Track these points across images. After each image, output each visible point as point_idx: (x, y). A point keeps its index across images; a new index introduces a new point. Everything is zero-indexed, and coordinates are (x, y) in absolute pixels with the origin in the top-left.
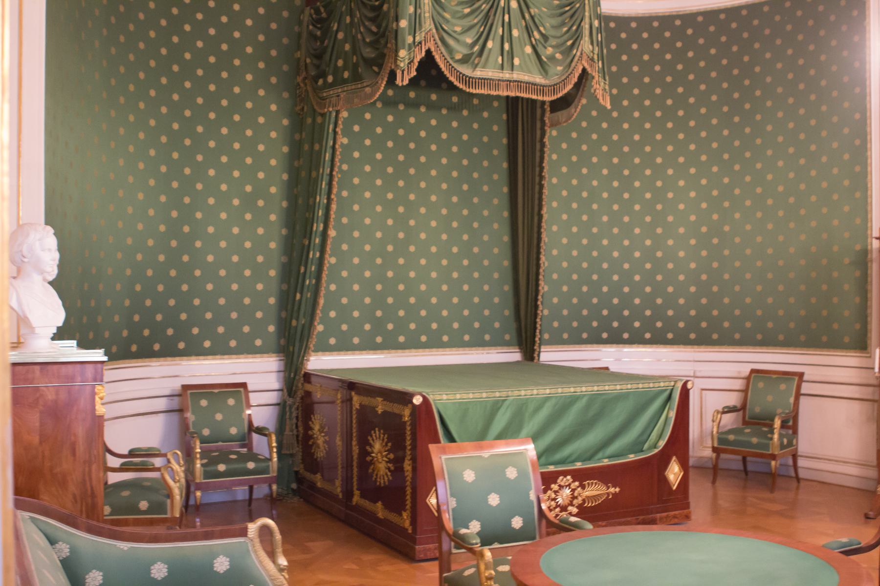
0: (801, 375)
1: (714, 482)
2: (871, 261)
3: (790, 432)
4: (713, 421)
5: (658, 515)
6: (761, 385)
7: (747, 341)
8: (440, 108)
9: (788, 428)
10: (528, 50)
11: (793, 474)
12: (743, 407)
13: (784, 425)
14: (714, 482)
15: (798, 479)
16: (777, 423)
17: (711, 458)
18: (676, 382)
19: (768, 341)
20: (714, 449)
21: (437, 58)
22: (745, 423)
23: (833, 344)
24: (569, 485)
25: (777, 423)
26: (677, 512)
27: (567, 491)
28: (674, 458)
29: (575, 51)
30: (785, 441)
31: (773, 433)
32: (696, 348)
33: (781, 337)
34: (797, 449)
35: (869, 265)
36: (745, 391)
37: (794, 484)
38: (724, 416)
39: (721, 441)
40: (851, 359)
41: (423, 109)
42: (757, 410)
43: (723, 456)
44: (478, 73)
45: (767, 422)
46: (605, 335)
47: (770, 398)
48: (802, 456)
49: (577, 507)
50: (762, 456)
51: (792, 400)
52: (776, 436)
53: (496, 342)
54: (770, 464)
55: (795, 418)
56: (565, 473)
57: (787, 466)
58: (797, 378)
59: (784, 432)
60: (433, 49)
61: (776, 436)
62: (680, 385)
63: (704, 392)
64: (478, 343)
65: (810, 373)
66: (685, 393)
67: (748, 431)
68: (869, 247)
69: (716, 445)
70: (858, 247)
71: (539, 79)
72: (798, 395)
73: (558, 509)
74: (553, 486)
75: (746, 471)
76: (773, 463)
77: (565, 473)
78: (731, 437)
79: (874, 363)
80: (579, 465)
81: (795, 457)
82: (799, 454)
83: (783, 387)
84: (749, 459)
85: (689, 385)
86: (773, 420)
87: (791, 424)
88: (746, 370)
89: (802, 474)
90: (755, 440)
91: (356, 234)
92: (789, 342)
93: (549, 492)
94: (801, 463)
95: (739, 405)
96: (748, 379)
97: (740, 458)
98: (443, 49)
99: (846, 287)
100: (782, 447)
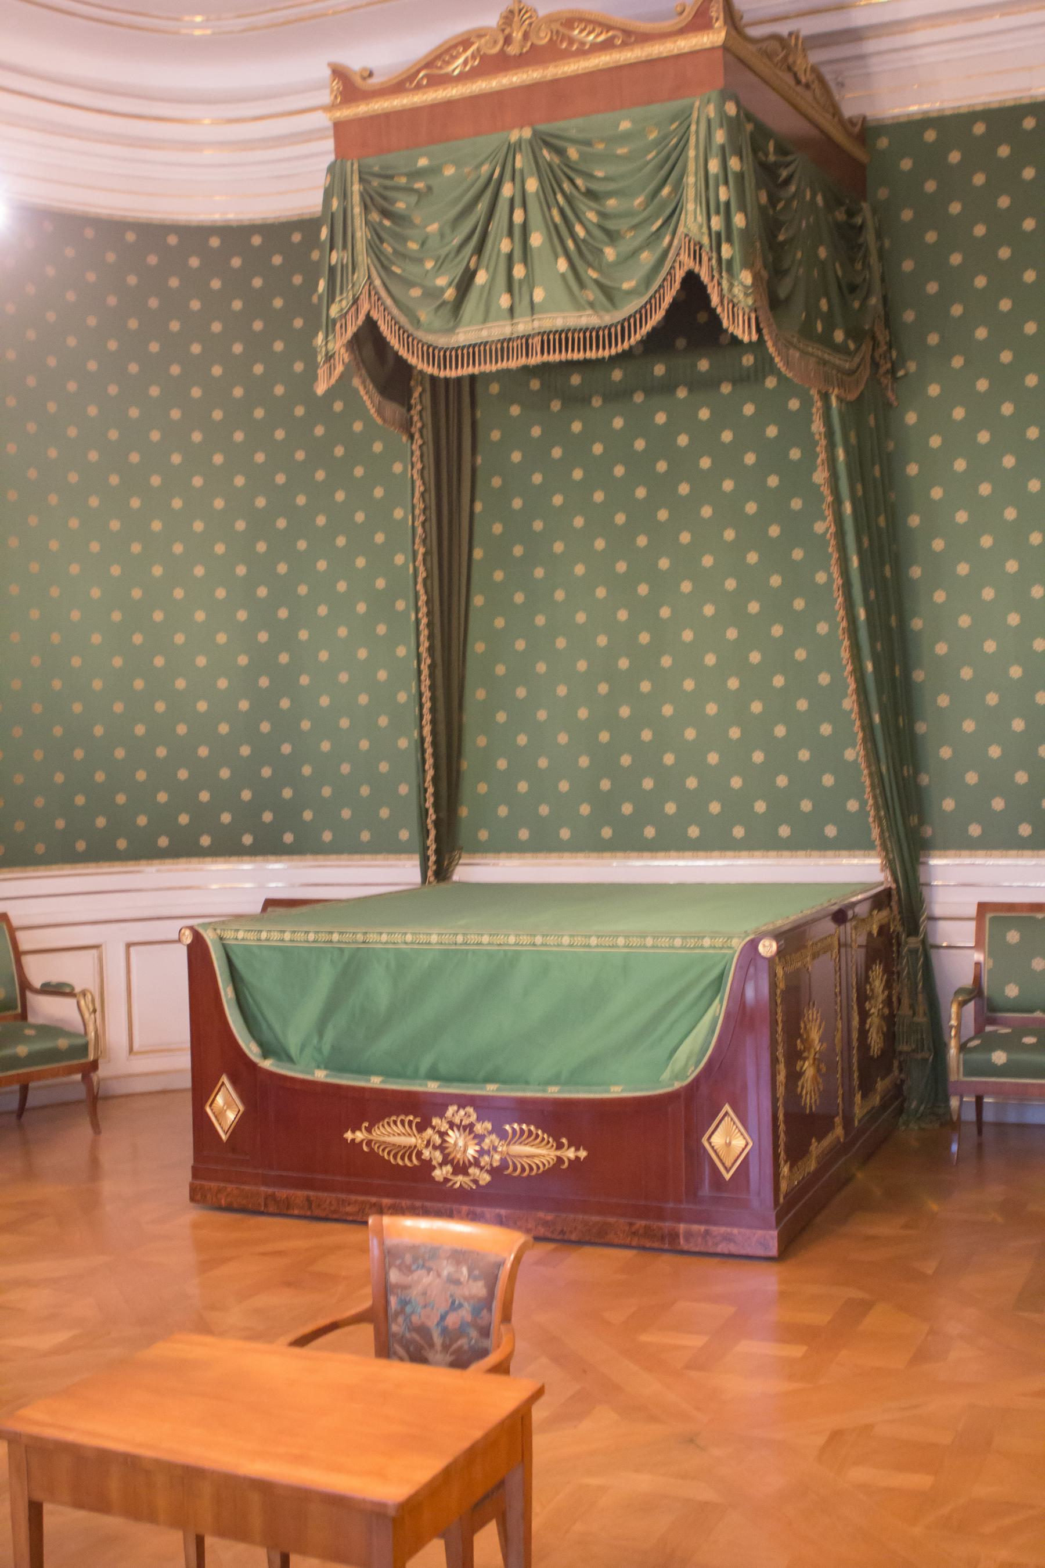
5: (682, 1227)
8: (718, 385)
10: (562, 265)
21: (384, 328)
24: (471, 1126)
26: (735, 1231)
27: (453, 1137)
29: (667, 240)
41: (682, 393)
44: (464, 336)
46: (163, 842)
49: (487, 1171)
53: (851, 842)
60: (375, 315)
64: (808, 840)
71: (587, 319)
73: (449, 1168)
74: (435, 1121)
77: (463, 1101)
91: (561, 643)
93: (429, 1131)
98: (395, 311)
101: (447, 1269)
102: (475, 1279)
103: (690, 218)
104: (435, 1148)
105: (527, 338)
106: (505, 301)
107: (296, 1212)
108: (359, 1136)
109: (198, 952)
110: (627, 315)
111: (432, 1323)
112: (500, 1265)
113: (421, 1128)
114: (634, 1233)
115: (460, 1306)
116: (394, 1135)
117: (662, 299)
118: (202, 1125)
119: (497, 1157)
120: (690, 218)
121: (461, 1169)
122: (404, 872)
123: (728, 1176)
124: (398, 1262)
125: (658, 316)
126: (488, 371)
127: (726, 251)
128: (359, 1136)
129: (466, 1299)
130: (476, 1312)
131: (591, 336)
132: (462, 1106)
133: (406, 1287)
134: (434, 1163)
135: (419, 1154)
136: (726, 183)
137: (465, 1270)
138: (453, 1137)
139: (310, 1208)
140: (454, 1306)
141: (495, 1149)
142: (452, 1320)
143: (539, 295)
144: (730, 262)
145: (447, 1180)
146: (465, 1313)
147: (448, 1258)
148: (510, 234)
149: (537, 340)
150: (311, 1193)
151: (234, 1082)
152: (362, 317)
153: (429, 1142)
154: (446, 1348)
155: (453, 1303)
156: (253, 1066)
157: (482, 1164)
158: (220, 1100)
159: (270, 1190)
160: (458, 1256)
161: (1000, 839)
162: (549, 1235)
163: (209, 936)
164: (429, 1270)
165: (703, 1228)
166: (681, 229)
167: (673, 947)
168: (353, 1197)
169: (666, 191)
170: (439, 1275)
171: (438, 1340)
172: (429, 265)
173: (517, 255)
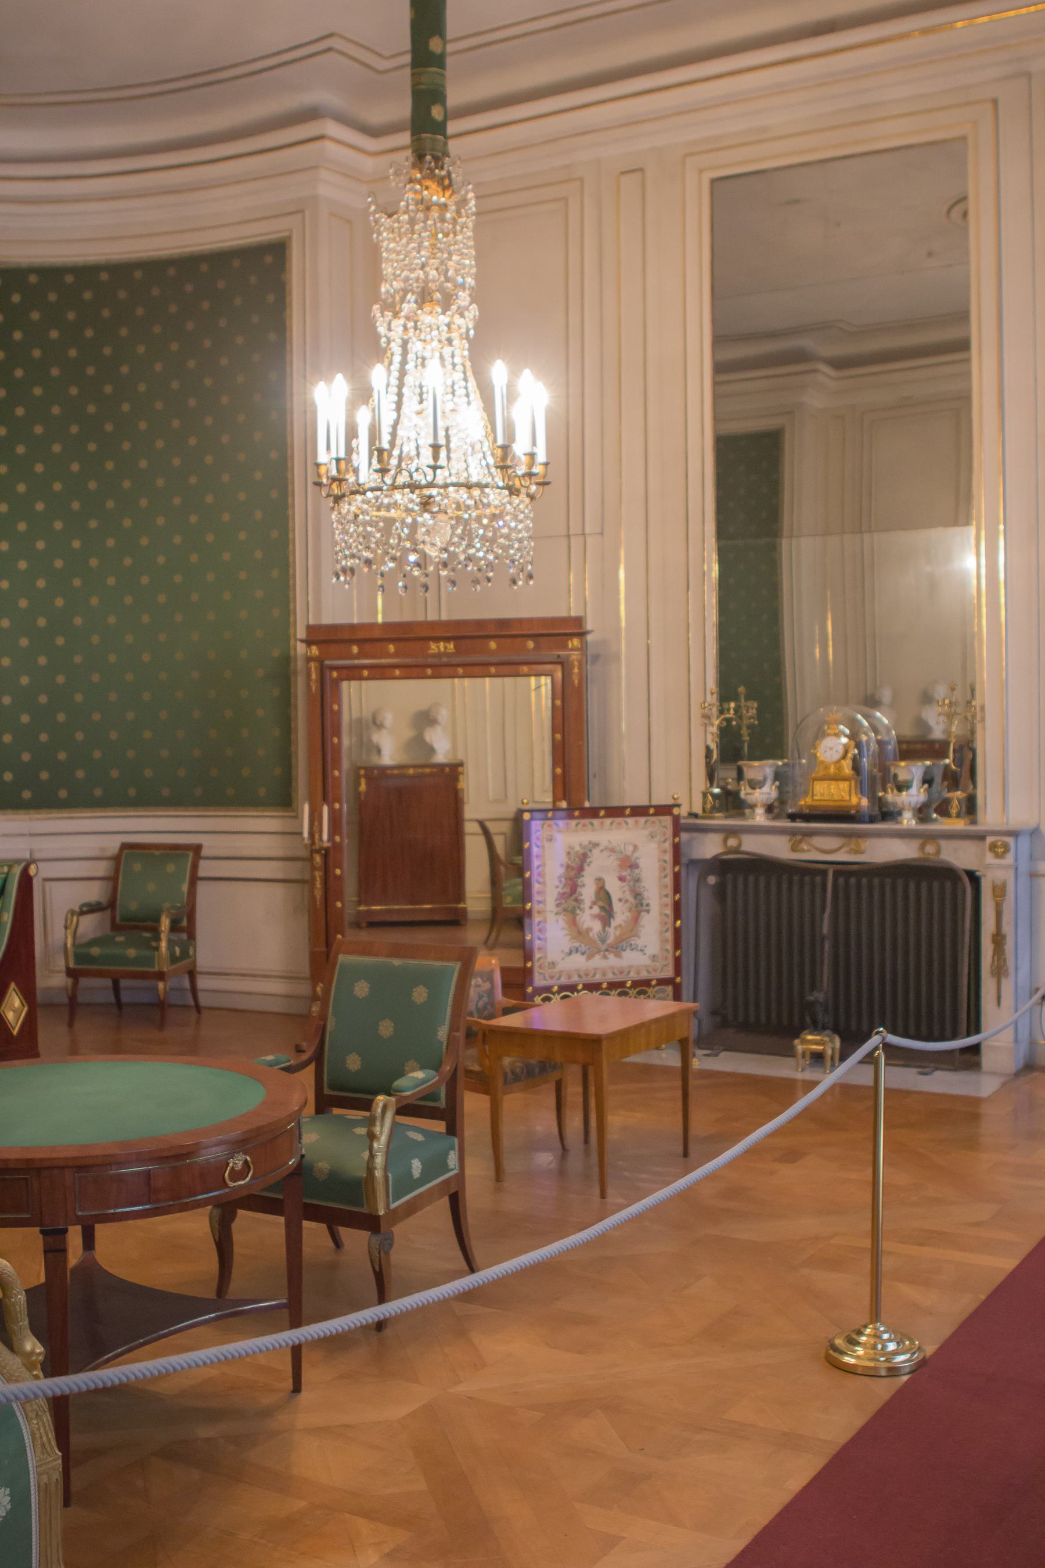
0: (197, 849)
1: (70, 1024)
2: (295, 673)
3: (184, 936)
4: (66, 928)
6: (137, 867)
7: (114, 799)
9: (181, 930)
11: (192, 1003)
12: (112, 904)
13: (174, 927)
14: (70, 1024)
15: (198, 1008)
16: (165, 923)
17: (66, 989)
18: (10, 867)
19: (146, 799)
20: (70, 973)
22: (115, 927)
23: (241, 798)
25: (165, 923)
28: (13, 985)
30: (177, 950)
31: (158, 939)
32: (34, 815)
33: (166, 792)
34: (194, 962)
35: (292, 679)
36: (113, 879)
37: (193, 1015)
38: (83, 919)
39: (79, 958)
40: (269, 822)
42: (133, 906)
43: (84, 982)
45: (149, 924)
47: (151, 887)
48: (202, 973)
50: (144, 976)
51: (185, 888)
52: (164, 944)
54: (156, 988)
55: (191, 916)
57: (181, 990)
58: (191, 854)
59: (174, 937)
61: (164, 944)
62: (17, 871)
63: (48, 884)
65: (210, 845)
66: (26, 883)
67: (120, 939)
68: (292, 653)
69: (72, 965)
70: (276, 653)
72: (194, 879)
75: (119, 1004)
76: (161, 985)
78: (95, 951)
79: (302, 826)
81: (192, 974)
82: (198, 969)
83: (171, 868)
84: (124, 983)
85: (32, 871)
86: (157, 920)
87: (185, 924)
88: (113, 845)
89: (204, 1000)
90: (132, 953)
92: (178, 799)
94: (202, 983)
95: (104, 901)
96: (117, 859)
97: (108, 982)
99: (260, 713)
100: (174, 959)
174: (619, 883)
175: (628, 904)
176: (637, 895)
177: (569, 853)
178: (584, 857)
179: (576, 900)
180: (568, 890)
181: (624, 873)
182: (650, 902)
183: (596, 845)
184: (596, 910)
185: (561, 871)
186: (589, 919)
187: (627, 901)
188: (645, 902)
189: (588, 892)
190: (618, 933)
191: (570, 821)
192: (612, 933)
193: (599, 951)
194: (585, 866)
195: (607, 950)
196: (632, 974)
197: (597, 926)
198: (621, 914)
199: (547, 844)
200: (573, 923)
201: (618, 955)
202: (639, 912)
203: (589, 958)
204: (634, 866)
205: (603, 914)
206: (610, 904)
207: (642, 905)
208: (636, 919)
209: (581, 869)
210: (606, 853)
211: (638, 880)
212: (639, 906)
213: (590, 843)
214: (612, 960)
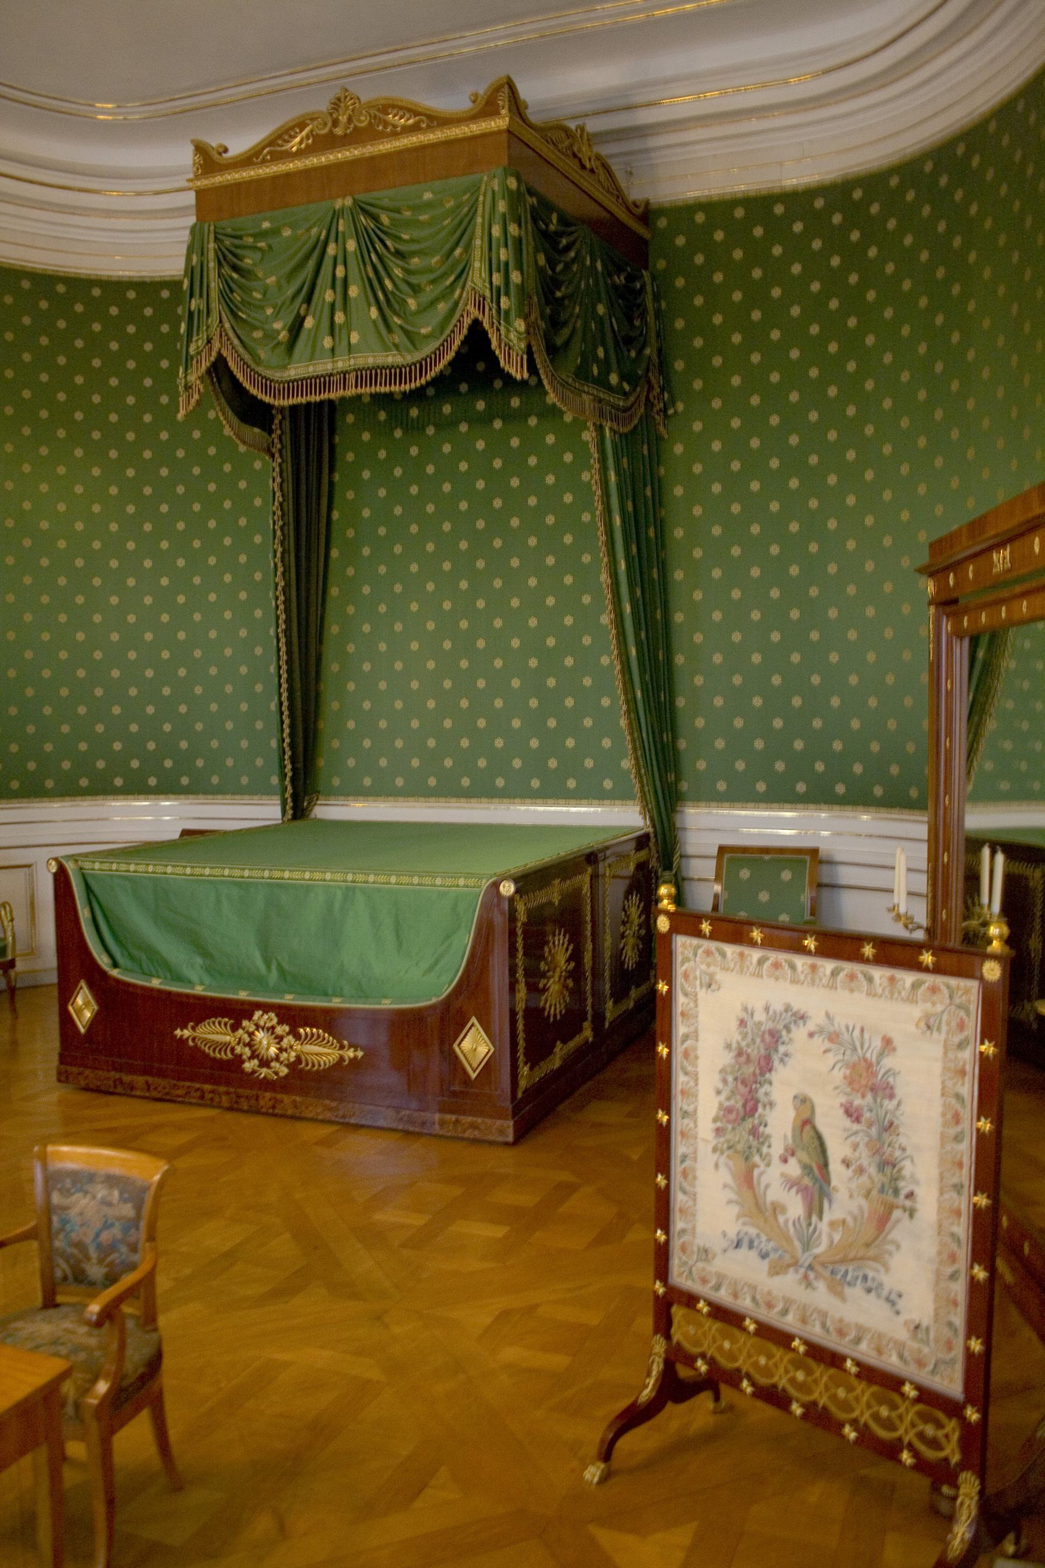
10: (374, 313)
21: (232, 365)
24: (273, 1028)
26: (480, 1120)
27: (260, 1035)
44: (294, 372)
49: (287, 1066)
56: (266, 1008)
60: (225, 353)
71: (392, 359)
73: (256, 1062)
74: (245, 1023)
77: (266, 1008)
80: (288, 999)
93: (240, 1031)
98: (241, 350)
101: (101, 1192)
102: (125, 1201)
103: (477, 274)
104: (245, 1045)
105: (345, 373)
106: (327, 343)
107: (138, 1093)
108: (186, 1033)
109: (61, 879)
110: (424, 356)
111: (88, 1240)
112: (145, 1189)
113: (235, 1028)
114: (401, 1120)
115: (112, 1225)
116: (213, 1035)
117: (452, 342)
118: (66, 1021)
119: (293, 1054)
120: (477, 274)
121: (265, 1063)
122: (268, 811)
123: (473, 1076)
124: (59, 1186)
125: (450, 356)
126: (313, 400)
127: (504, 303)
128: (186, 1033)
129: (118, 1219)
130: (126, 1230)
131: (396, 373)
132: (266, 1012)
133: (66, 1208)
134: (244, 1057)
135: (233, 1050)
136: (506, 246)
137: (116, 1193)
138: (260, 1035)
139: (148, 1090)
140: (107, 1226)
141: (291, 1047)
142: (105, 1237)
143: (355, 337)
144: (507, 313)
145: (254, 1072)
146: (116, 1232)
147: (103, 1182)
148: (333, 287)
149: (353, 375)
150: (150, 1079)
151: (91, 986)
152: (214, 354)
153: (240, 1039)
154: (101, 1261)
155: (106, 1222)
156: (103, 974)
157: (282, 1059)
158: (80, 1001)
159: (117, 1075)
160: (111, 1181)
161: (741, 794)
162: (333, 1119)
163: (70, 867)
164: (86, 1193)
165: (454, 1117)
166: (469, 283)
167: (435, 885)
168: (182, 1083)
169: (458, 252)
170: (94, 1197)
171: (93, 1253)
172: (269, 311)
173: (339, 304)
174: (847, 1123)
175: (864, 1179)
176: (888, 1165)
177: (742, 1023)
178: (774, 1038)
179: (754, 1132)
180: (738, 1103)
181: (858, 1102)
182: (920, 1192)
183: (801, 1017)
184: (793, 1168)
185: (727, 1058)
186: (777, 1177)
187: (861, 1170)
188: (905, 1187)
189: (780, 1123)
190: (837, 1237)
191: (747, 950)
192: (826, 1237)
193: (795, 1264)
194: (776, 1059)
195: (810, 1267)
196: (864, 1346)
197: (795, 1207)
198: (847, 1199)
199: (702, 994)
200: (747, 1179)
201: (837, 1288)
202: (890, 1208)
203: (776, 1270)
204: (884, 1090)
205: (807, 1181)
206: (825, 1165)
207: (896, 1192)
208: (882, 1221)
209: (766, 1065)
210: (817, 1040)
211: (890, 1127)
212: (890, 1198)
213: (788, 1008)
214: (821, 1296)
